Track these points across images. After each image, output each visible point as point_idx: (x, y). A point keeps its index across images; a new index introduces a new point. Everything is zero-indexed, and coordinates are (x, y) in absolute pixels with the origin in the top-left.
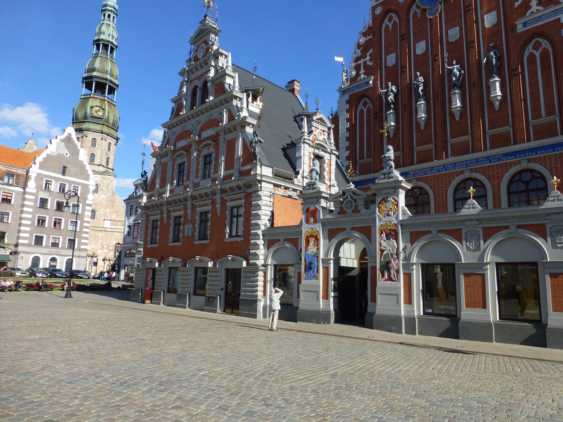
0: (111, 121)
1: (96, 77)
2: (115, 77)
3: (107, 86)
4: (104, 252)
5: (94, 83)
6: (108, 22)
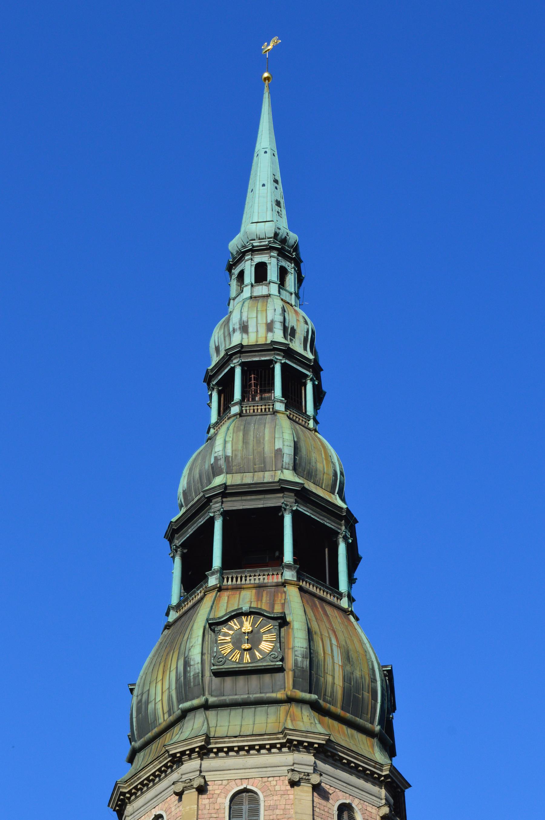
0: (334, 678)
1: (225, 492)
2: (327, 479)
5: (218, 525)
6: (261, 290)
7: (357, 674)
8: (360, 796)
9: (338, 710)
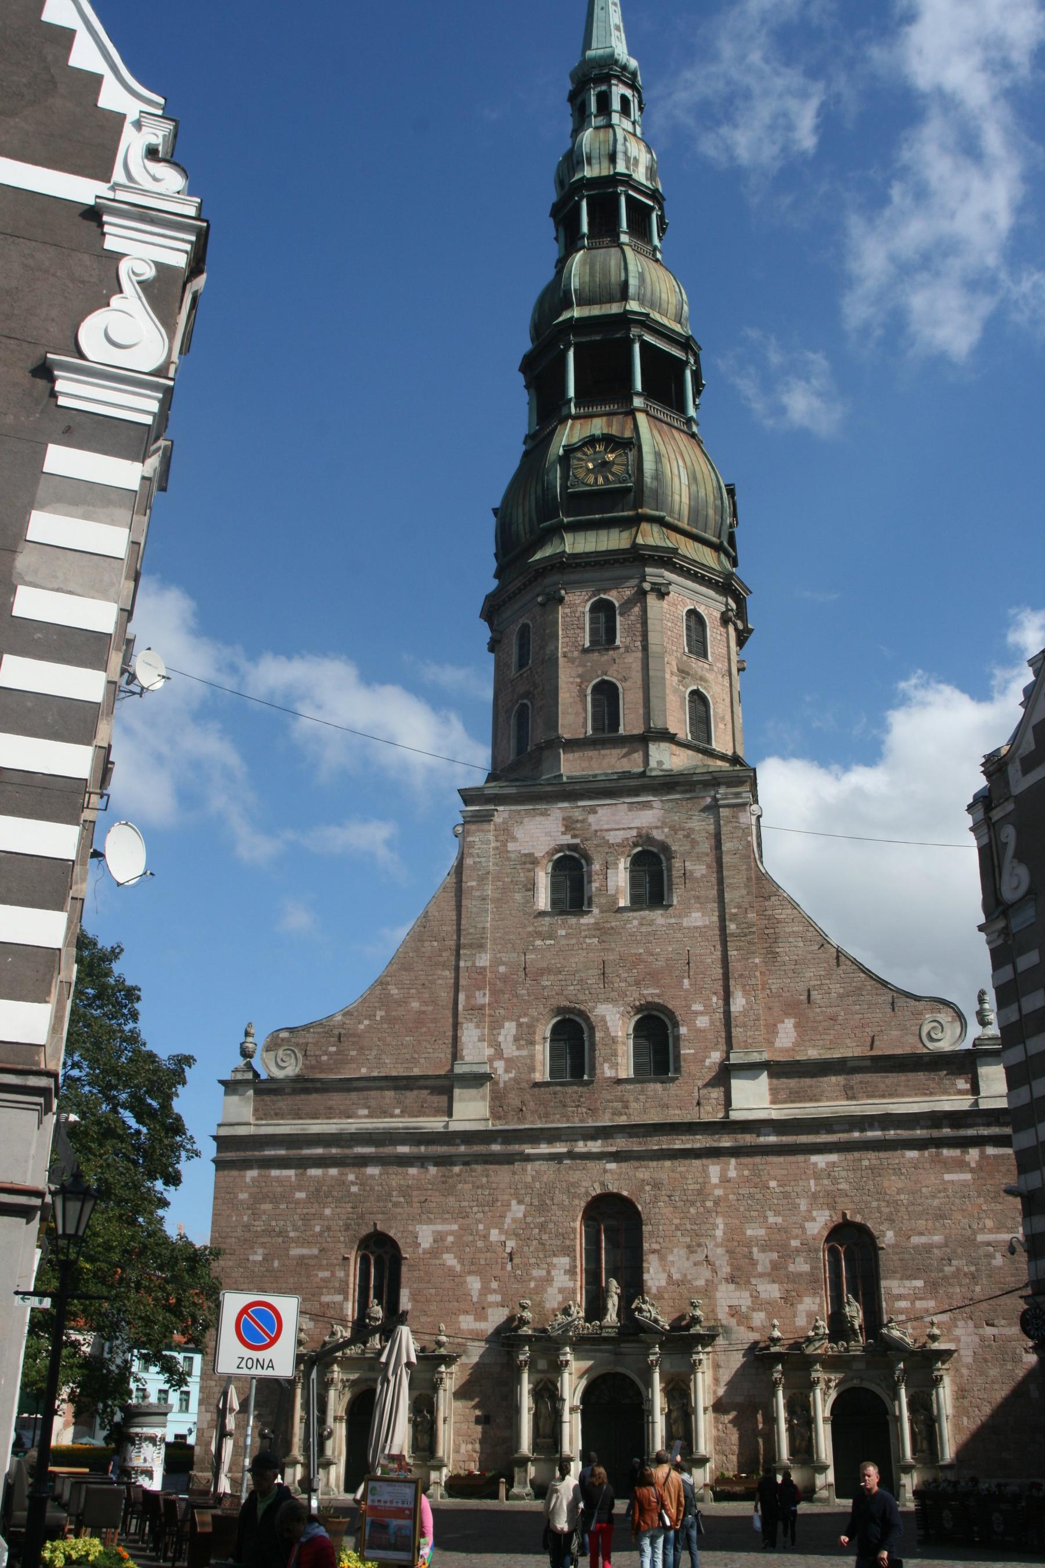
2: (672, 310)
3: (637, 347)
4: (758, 1303)
6: (600, 121)
7: (702, 494)
8: (705, 602)
9: (684, 525)
